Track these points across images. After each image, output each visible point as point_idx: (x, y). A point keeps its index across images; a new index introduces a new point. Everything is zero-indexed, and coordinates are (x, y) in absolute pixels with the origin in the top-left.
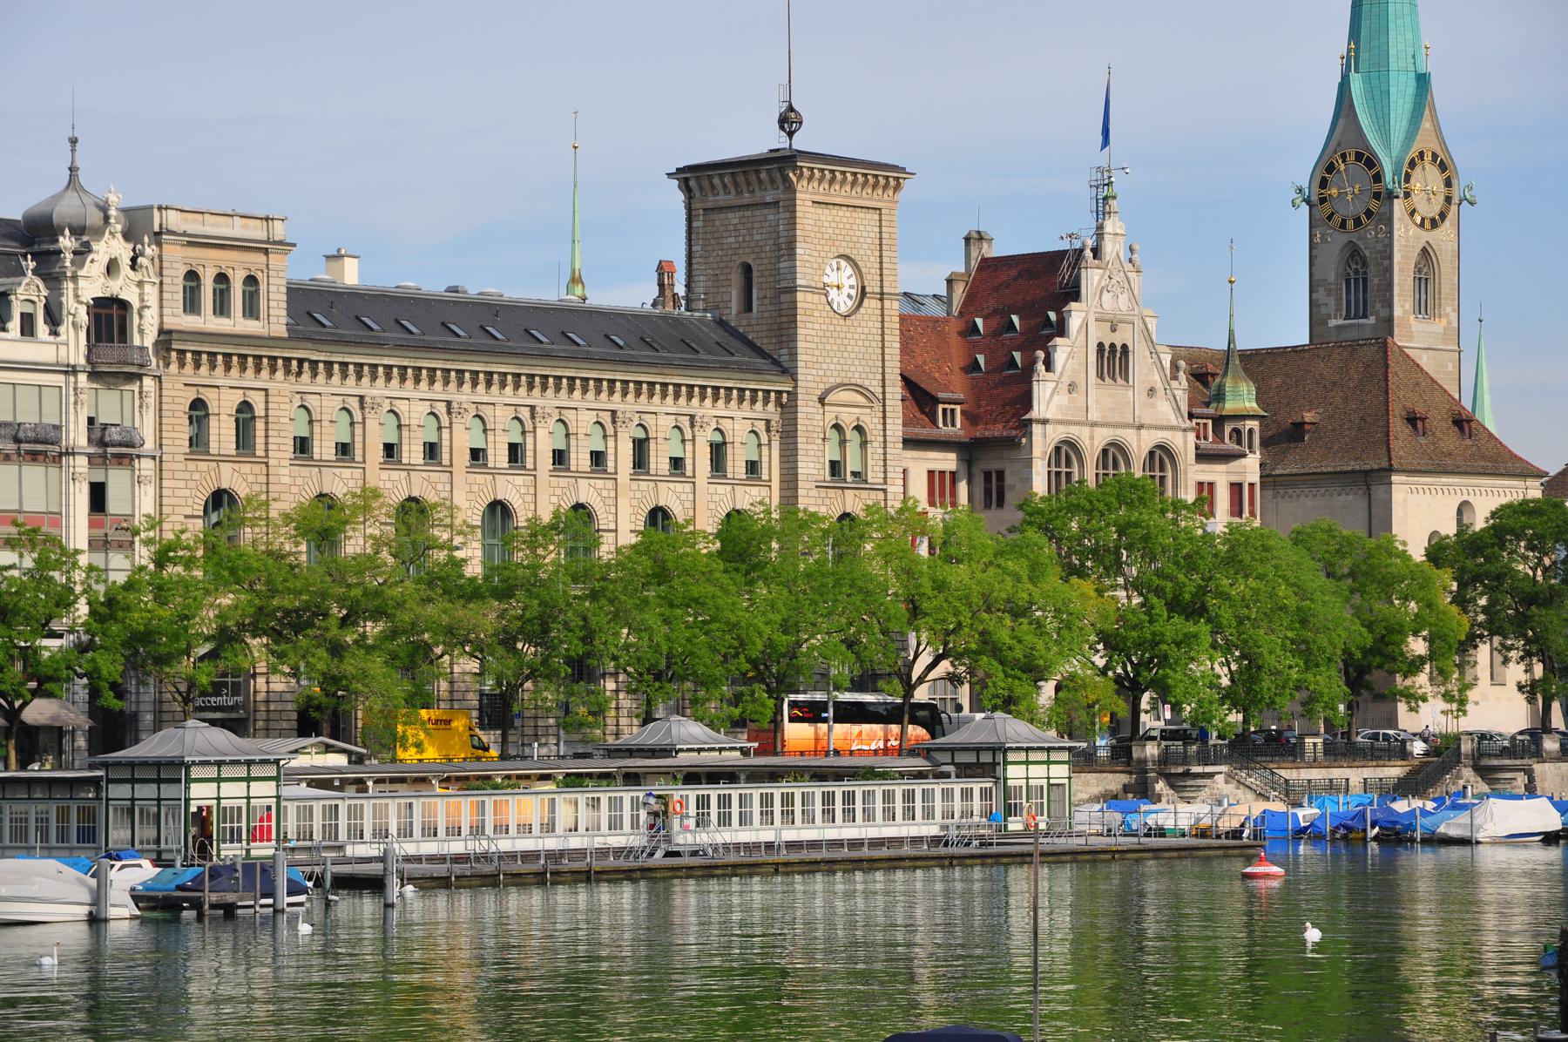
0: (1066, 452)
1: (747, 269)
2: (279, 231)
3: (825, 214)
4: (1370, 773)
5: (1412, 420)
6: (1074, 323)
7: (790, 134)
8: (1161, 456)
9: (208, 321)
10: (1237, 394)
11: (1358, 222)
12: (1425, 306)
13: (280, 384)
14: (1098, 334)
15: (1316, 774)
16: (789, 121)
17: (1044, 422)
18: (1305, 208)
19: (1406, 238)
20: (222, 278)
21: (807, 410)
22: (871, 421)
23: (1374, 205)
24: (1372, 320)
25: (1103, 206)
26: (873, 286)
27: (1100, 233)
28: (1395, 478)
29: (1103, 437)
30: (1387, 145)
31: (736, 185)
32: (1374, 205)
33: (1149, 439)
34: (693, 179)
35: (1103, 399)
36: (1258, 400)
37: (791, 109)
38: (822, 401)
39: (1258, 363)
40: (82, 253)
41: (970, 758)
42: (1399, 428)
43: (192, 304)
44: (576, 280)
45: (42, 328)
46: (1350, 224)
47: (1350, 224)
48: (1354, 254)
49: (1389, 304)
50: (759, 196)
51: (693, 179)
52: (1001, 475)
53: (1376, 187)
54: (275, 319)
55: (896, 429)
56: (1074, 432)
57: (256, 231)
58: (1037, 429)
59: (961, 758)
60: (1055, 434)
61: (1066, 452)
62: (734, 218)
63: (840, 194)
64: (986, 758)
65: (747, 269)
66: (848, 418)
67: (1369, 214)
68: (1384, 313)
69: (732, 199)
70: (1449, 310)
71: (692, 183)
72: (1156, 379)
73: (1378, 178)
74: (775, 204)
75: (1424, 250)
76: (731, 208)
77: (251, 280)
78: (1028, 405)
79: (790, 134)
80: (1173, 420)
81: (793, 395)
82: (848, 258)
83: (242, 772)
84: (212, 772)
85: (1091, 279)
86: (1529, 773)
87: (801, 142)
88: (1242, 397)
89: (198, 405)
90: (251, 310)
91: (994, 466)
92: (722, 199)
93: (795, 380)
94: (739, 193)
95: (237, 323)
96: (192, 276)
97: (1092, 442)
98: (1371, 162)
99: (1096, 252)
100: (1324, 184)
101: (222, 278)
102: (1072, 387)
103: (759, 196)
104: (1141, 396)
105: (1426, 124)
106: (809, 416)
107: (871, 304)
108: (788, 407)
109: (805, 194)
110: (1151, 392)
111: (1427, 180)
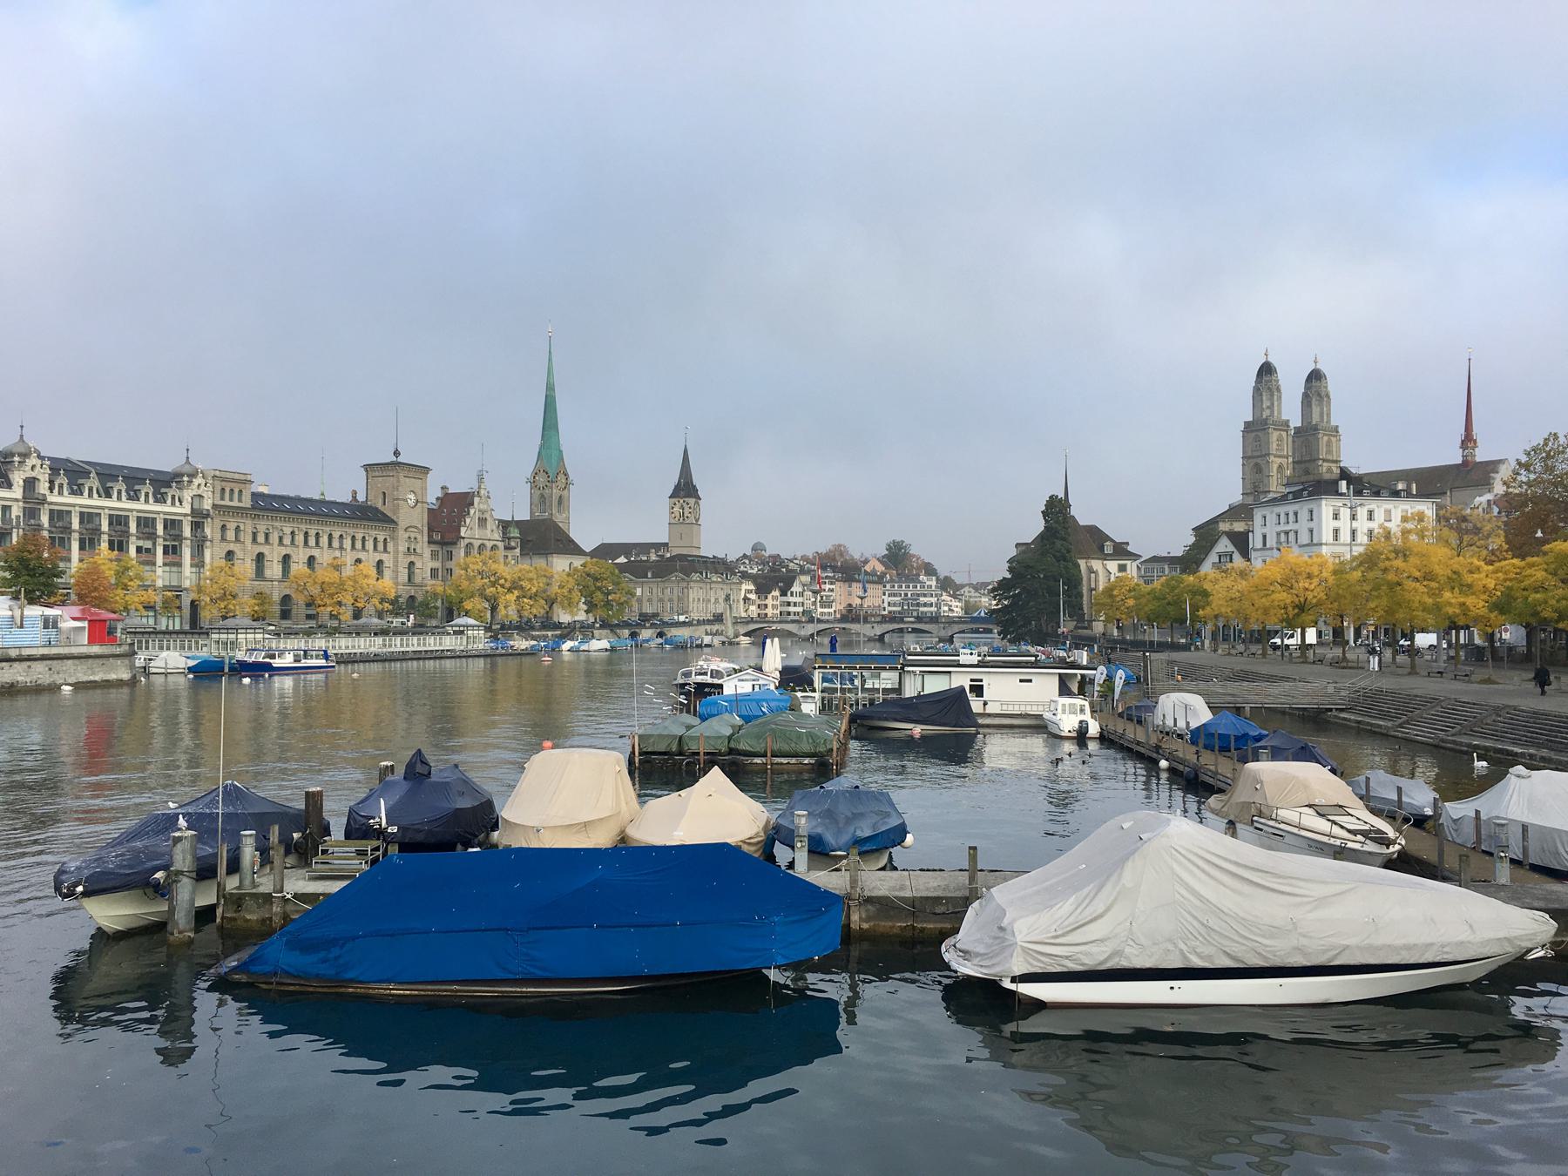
1: (384, 493)
2: (249, 478)
3: (407, 480)
4: (552, 633)
6: (472, 511)
8: (494, 548)
9: (227, 502)
10: (514, 532)
11: (543, 488)
13: (249, 522)
15: (537, 633)
16: (397, 453)
20: (232, 490)
22: (419, 537)
23: (548, 484)
25: (481, 480)
27: (479, 488)
39: (519, 524)
40: (190, 482)
41: (458, 629)
43: (222, 499)
44: (323, 494)
45: (177, 503)
48: (542, 496)
51: (368, 468)
52: (451, 552)
54: (247, 502)
55: (426, 539)
56: (472, 541)
57: (242, 477)
59: (454, 629)
60: (467, 541)
62: (380, 479)
64: (462, 629)
65: (384, 493)
66: (413, 535)
72: (494, 528)
74: (393, 476)
75: (560, 497)
77: (241, 491)
83: (253, 631)
84: (244, 631)
85: (476, 500)
86: (592, 632)
87: (400, 459)
88: (515, 533)
89: (224, 526)
90: (240, 501)
91: (449, 549)
92: (377, 474)
95: (235, 503)
96: (223, 489)
98: (547, 473)
100: (534, 477)
101: (232, 490)
103: (388, 474)
110: (492, 531)
111: (561, 478)
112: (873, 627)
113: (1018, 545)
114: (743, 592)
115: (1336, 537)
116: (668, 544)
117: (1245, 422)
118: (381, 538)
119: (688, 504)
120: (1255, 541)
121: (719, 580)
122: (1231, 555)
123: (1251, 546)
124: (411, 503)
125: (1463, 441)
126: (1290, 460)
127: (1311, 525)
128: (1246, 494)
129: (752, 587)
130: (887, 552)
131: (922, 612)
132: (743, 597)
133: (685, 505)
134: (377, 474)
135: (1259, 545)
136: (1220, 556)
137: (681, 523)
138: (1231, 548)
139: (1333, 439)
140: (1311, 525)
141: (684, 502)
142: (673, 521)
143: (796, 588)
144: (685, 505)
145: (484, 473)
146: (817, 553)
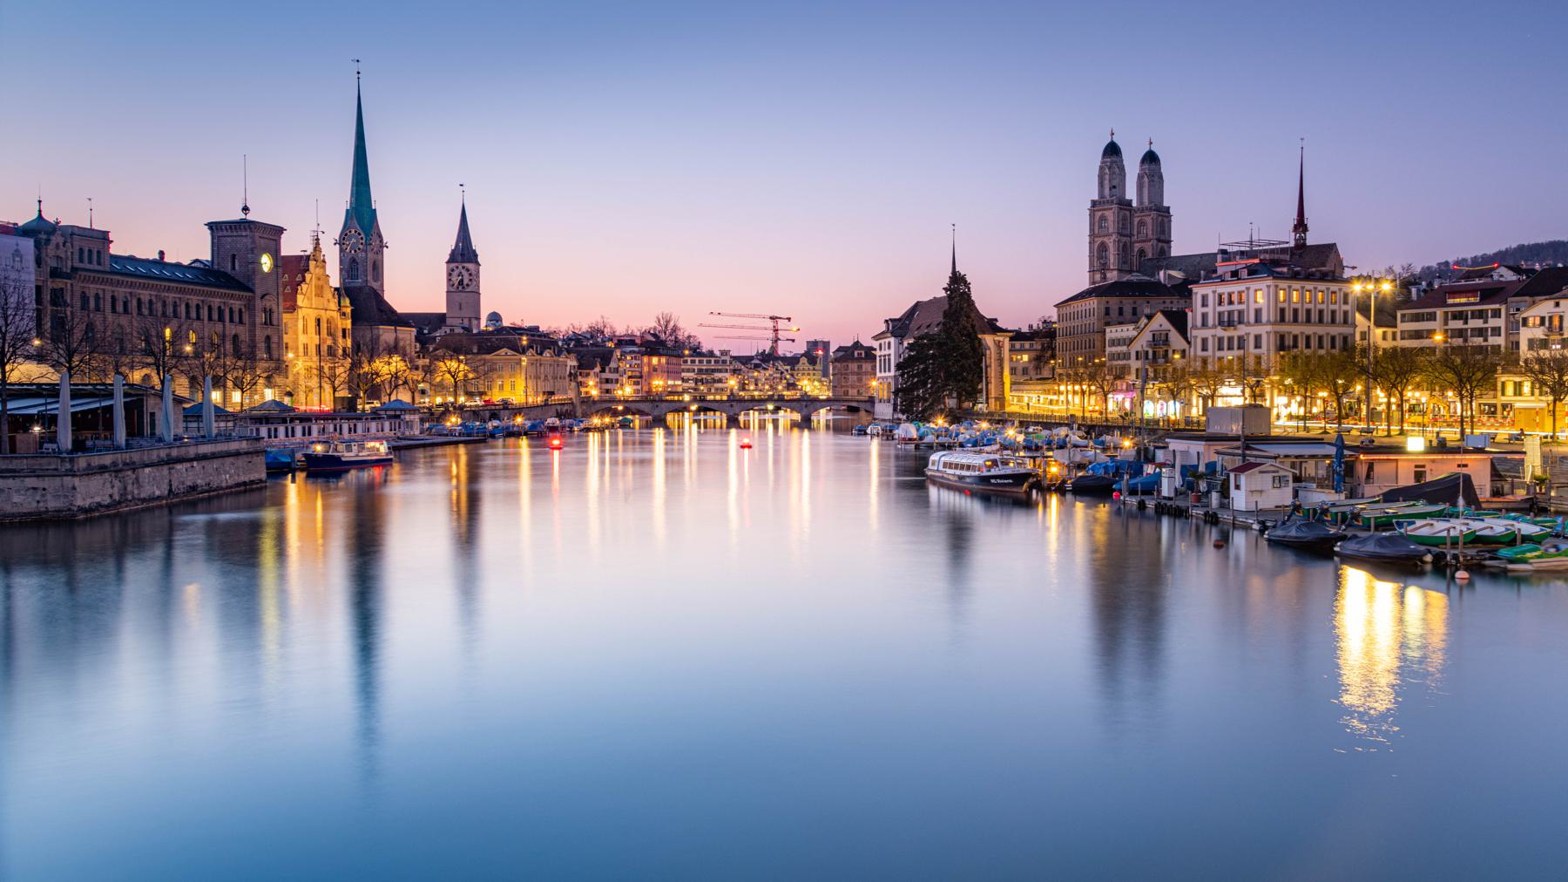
3: (262, 241)
7: (246, 214)
11: (355, 251)
18: (338, 246)
24: (360, 280)
50: (239, 233)
62: (229, 239)
67: (359, 249)
69: (229, 233)
76: (228, 236)
79: (246, 214)
87: (250, 217)
92: (225, 233)
94: (232, 232)
103: (239, 233)
116: (444, 315)
121: (548, 355)
132: (568, 373)
134: (225, 233)
137: (460, 291)
141: (463, 267)
142: (452, 289)
145: (320, 234)
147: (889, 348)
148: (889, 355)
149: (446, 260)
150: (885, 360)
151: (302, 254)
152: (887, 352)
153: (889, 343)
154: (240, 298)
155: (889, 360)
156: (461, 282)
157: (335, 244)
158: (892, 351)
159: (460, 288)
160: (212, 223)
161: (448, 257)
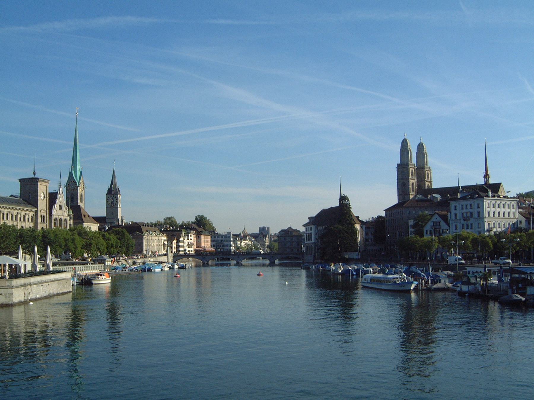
0: (56, 219)
3: (41, 186)
5: (84, 216)
6: (57, 201)
11: (73, 190)
12: (81, 201)
14: (59, 203)
16: (34, 173)
17: (54, 215)
18: (66, 188)
19: (79, 192)
21: (39, 213)
23: (76, 188)
24: (75, 203)
26: (45, 196)
28: (84, 223)
29: (60, 217)
30: (77, 180)
31: (29, 181)
32: (76, 188)
33: (65, 217)
34: (21, 180)
35: (60, 212)
36: (73, 213)
37: (35, 171)
38: (40, 212)
42: (83, 217)
46: (72, 190)
47: (72, 190)
48: (72, 194)
49: (77, 201)
53: (76, 186)
58: (53, 216)
61: (56, 219)
63: (43, 184)
66: (43, 214)
67: (75, 189)
68: (77, 202)
70: (83, 202)
71: (22, 181)
73: (76, 184)
78: (52, 213)
80: (66, 215)
81: (37, 211)
82: (43, 192)
85: (59, 196)
87: (36, 176)
93: (37, 208)
97: (58, 218)
98: (75, 183)
99: (59, 192)
102: (57, 211)
104: (63, 212)
105: (82, 178)
106: (39, 214)
107: (45, 198)
108: (36, 213)
109: (39, 183)
112: (239, 257)
113: (309, 218)
114: (163, 241)
115: (489, 215)
116: (105, 217)
117: (398, 164)
118: (14, 214)
119: (115, 197)
120: (451, 216)
121: (155, 235)
122: (439, 223)
123: (449, 218)
124: (42, 198)
125: (484, 175)
126: (416, 180)
127: (479, 210)
128: (400, 195)
129: (165, 239)
130: (195, 220)
131: (226, 249)
132: (163, 243)
133: (114, 198)
135: (453, 218)
136: (434, 223)
137: (112, 207)
138: (439, 219)
139: (429, 172)
140: (479, 210)
141: (114, 196)
142: (109, 206)
143: (182, 239)
144: (114, 198)
146: (157, 221)
147: (311, 230)
148: (311, 233)
149: (106, 193)
150: (309, 235)
151: (54, 192)
152: (310, 232)
153: (311, 228)
154: (32, 211)
155: (311, 236)
156: (112, 203)
157: (65, 187)
158: (313, 232)
159: (112, 205)
160: (22, 179)
161: (107, 192)
